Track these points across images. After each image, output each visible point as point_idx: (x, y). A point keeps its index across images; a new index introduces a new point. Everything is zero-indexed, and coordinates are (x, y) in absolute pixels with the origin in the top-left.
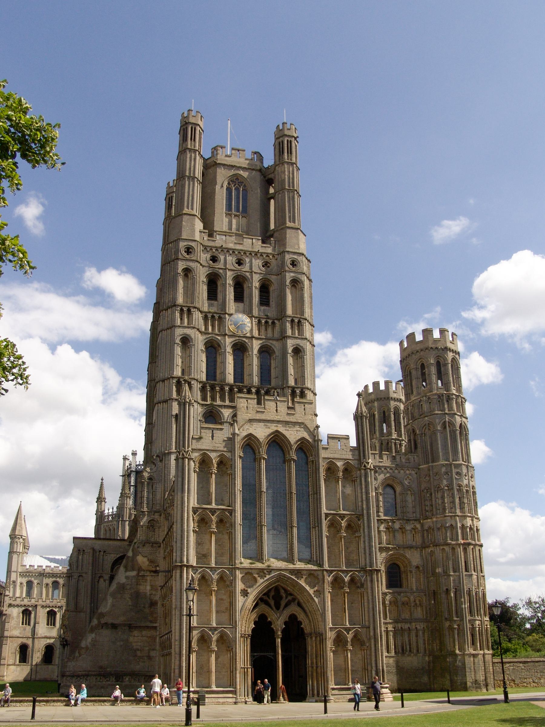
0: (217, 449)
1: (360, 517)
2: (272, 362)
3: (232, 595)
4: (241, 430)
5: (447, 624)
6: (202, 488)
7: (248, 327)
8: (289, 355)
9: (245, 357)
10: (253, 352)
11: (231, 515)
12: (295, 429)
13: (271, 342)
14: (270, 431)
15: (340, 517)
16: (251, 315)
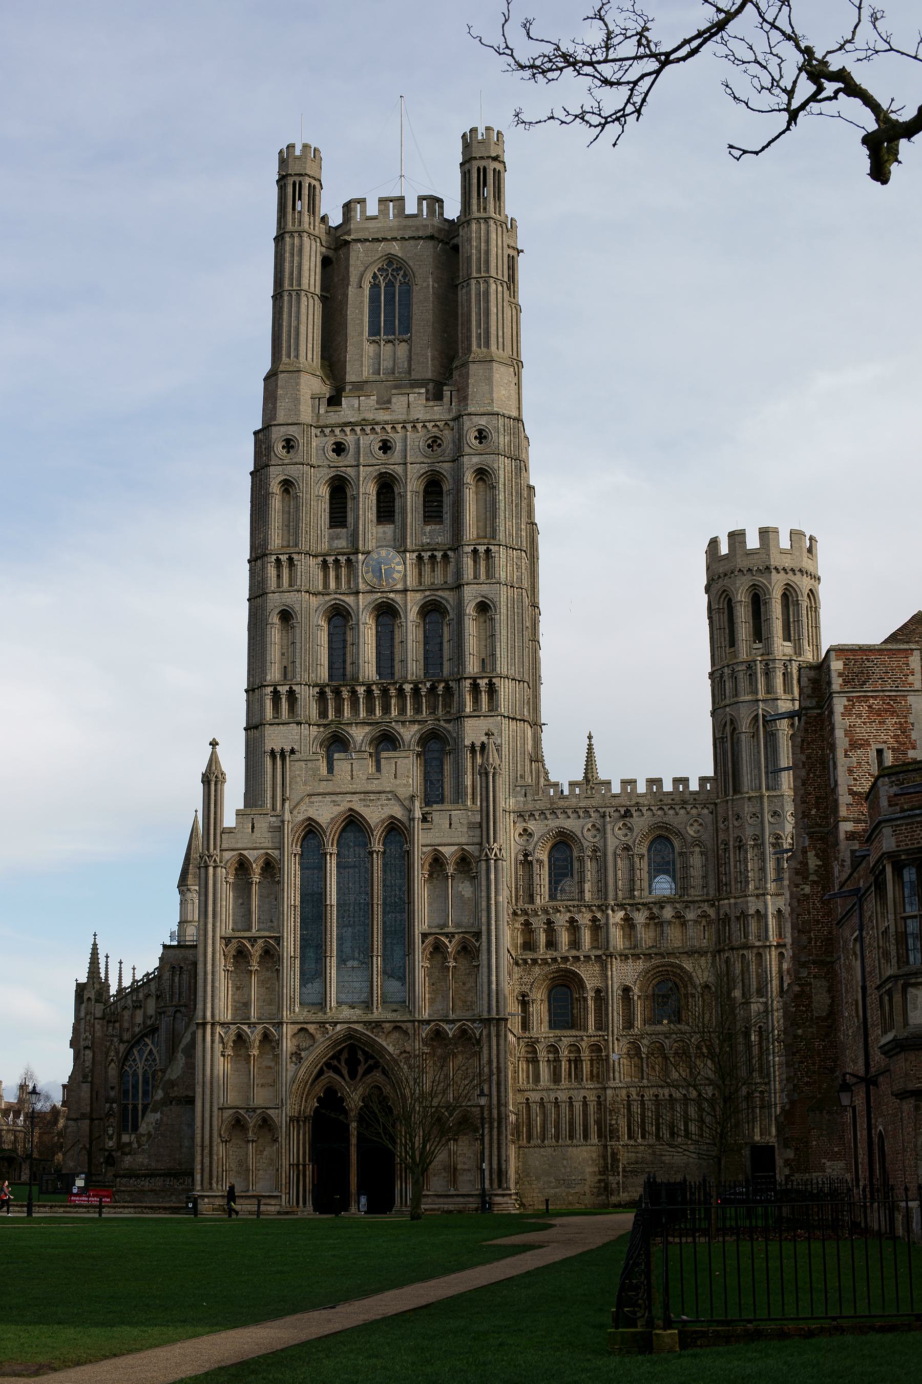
0: (258, 845)
1: (478, 935)
2: (446, 629)
3: (277, 1058)
4: (295, 812)
5: (744, 1091)
6: (242, 904)
7: (399, 572)
8: (466, 618)
9: (396, 627)
10: (406, 618)
11: (278, 944)
12: (379, 803)
13: (440, 593)
14: (341, 809)
15: (447, 937)
16: (402, 549)
